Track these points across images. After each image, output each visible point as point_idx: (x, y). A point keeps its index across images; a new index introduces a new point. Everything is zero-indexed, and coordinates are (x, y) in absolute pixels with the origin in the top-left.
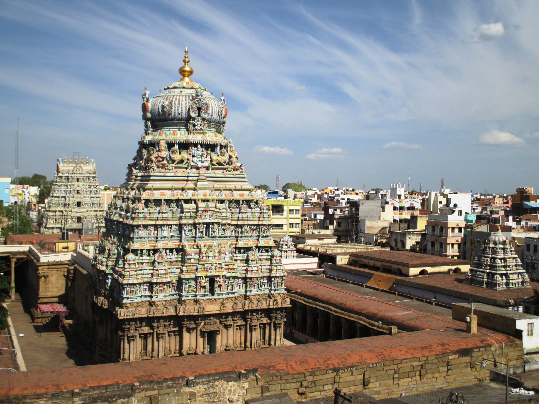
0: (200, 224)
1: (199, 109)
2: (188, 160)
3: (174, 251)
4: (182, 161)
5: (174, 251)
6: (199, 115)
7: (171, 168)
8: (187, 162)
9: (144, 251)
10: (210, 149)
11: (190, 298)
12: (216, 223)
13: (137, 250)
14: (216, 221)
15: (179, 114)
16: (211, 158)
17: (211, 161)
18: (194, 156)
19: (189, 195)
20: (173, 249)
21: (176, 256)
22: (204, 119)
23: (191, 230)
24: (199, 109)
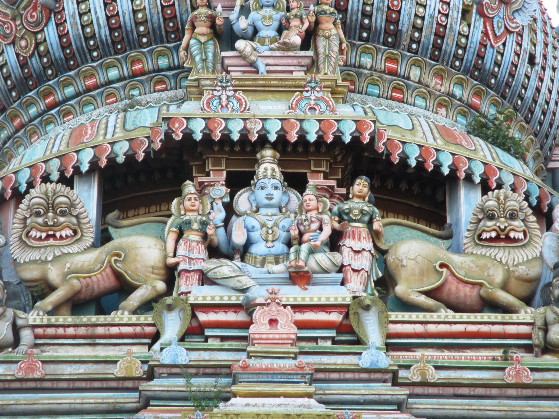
16: (381, 253)
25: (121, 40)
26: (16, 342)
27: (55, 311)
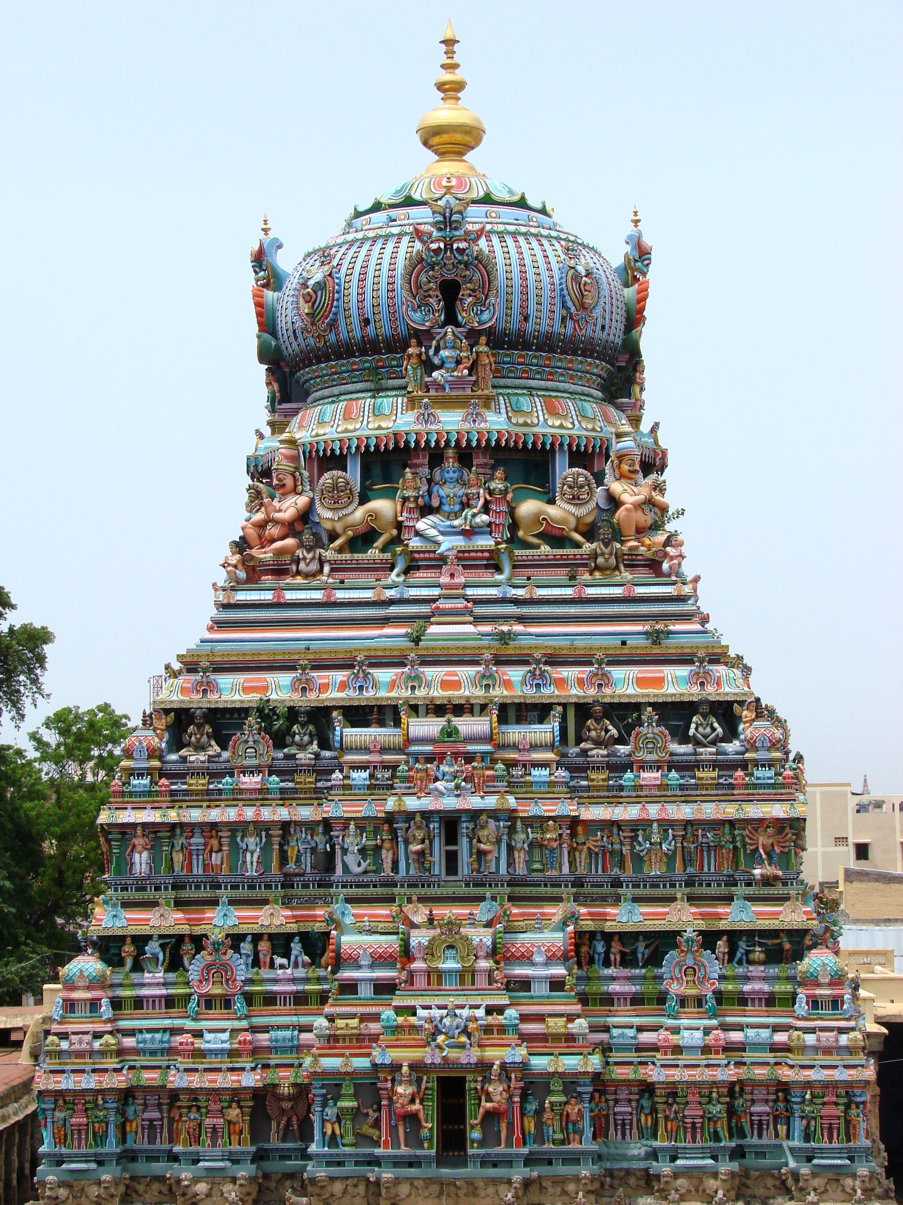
0: (409, 816)
1: (450, 291)
2: (399, 526)
3: (296, 947)
4: (364, 538)
5: (296, 947)
6: (451, 319)
7: (314, 566)
8: (397, 540)
9: (153, 947)
10: (499, 473)
11: (349, 1169)
12: (494, 814)
13: (122, 939)
14: (491, 802)
15: (367, 322)
17: (514, 526)
18: (426, 510)
19: (385, 685)
20: (289, 937)
21: (301, 973)
22: (473, 336)
23: (378, 849)
24: (450, 291)
25: (369, 347)
26: (321, 571)
27: (340, 550)
